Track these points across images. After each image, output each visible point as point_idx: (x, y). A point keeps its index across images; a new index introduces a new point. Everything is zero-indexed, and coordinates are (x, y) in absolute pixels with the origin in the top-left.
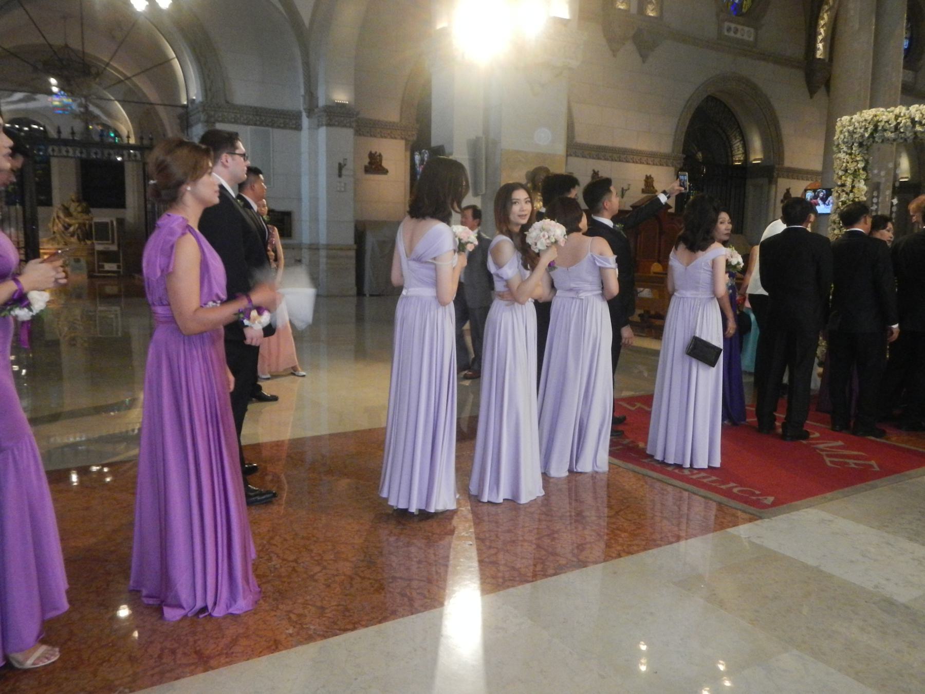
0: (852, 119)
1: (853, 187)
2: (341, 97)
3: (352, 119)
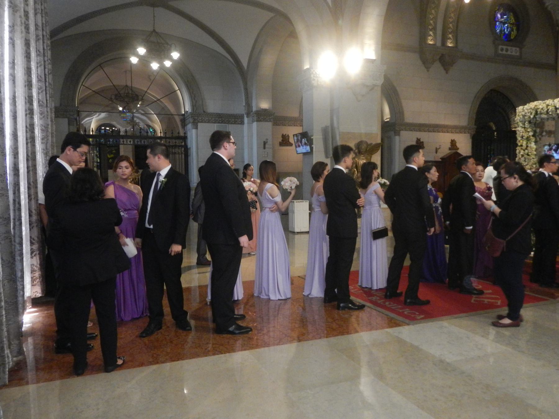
0: (524, 108)
1: (527, 146)
2: (265, 105)
3: (271, 117)
